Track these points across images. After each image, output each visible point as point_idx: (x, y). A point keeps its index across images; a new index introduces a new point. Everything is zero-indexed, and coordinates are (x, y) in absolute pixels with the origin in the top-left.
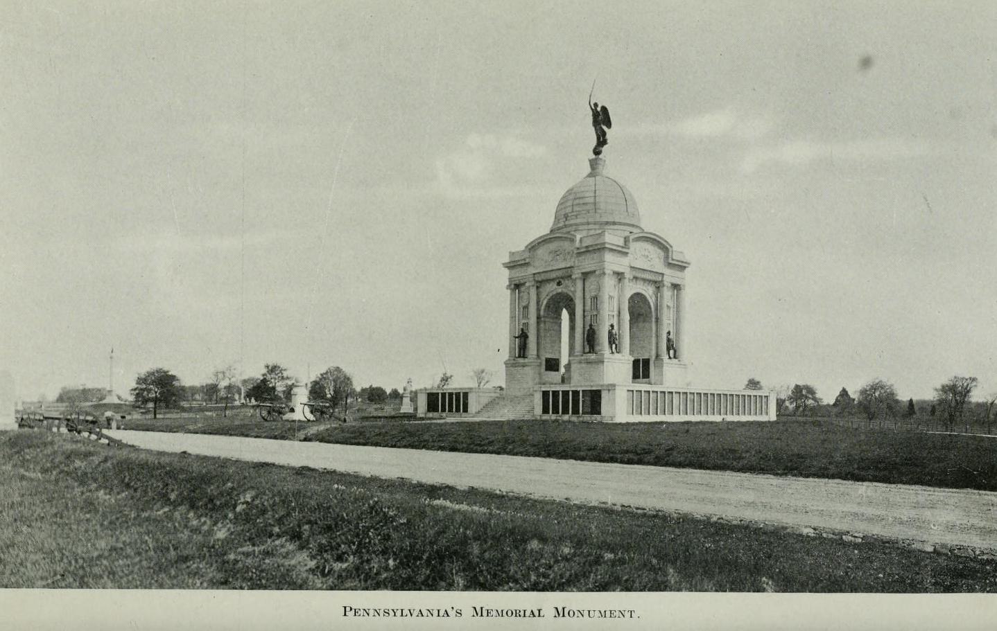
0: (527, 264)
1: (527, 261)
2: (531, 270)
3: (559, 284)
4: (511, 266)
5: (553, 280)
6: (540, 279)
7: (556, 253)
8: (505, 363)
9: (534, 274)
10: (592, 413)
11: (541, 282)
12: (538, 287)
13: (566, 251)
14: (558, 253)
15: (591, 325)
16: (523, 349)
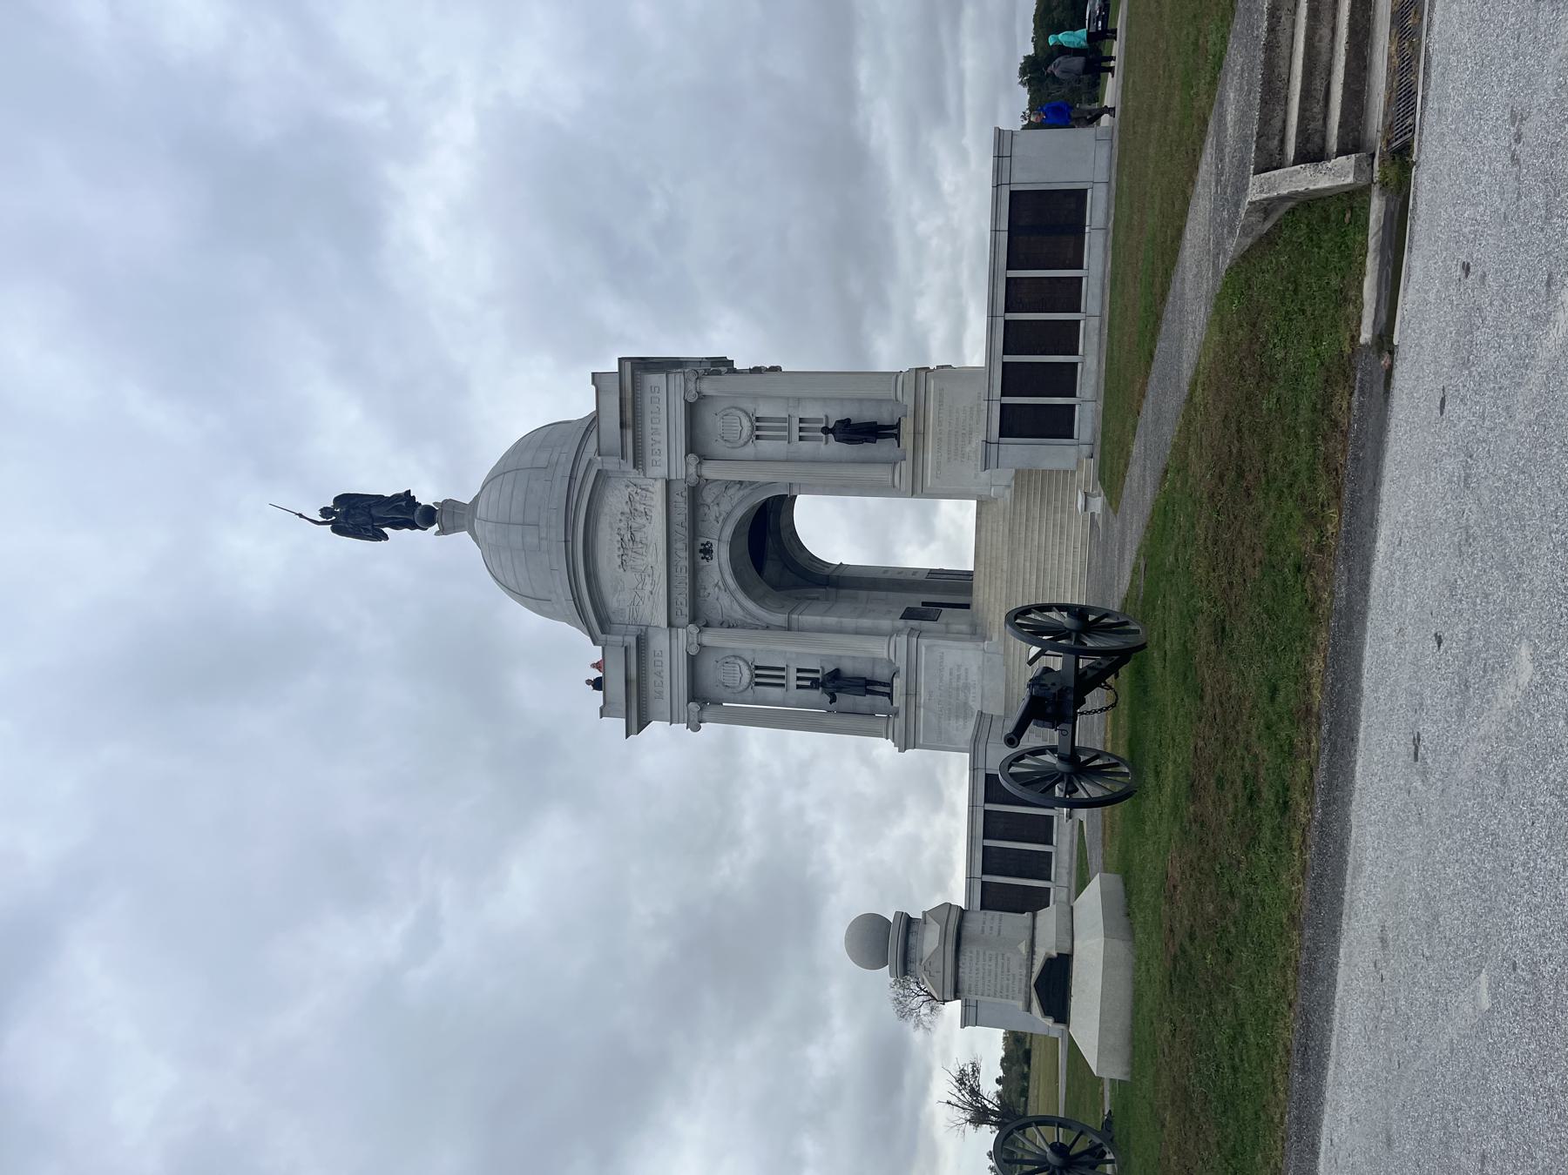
0: (642, 643)
1: (632, 641)
2: (660, 642)
3: (707, 551)
4: (638, 720)
5: (694, 572)
6: (686, 610)
7: (630, 542)
8: (903, 748)
9: (670, 625)
10: (1077, 229)
11: (694, 619)
12: (707, 625)
13: (627, 510)
14: (627, 537)
15: (826, 430)
16: (866, 685)
